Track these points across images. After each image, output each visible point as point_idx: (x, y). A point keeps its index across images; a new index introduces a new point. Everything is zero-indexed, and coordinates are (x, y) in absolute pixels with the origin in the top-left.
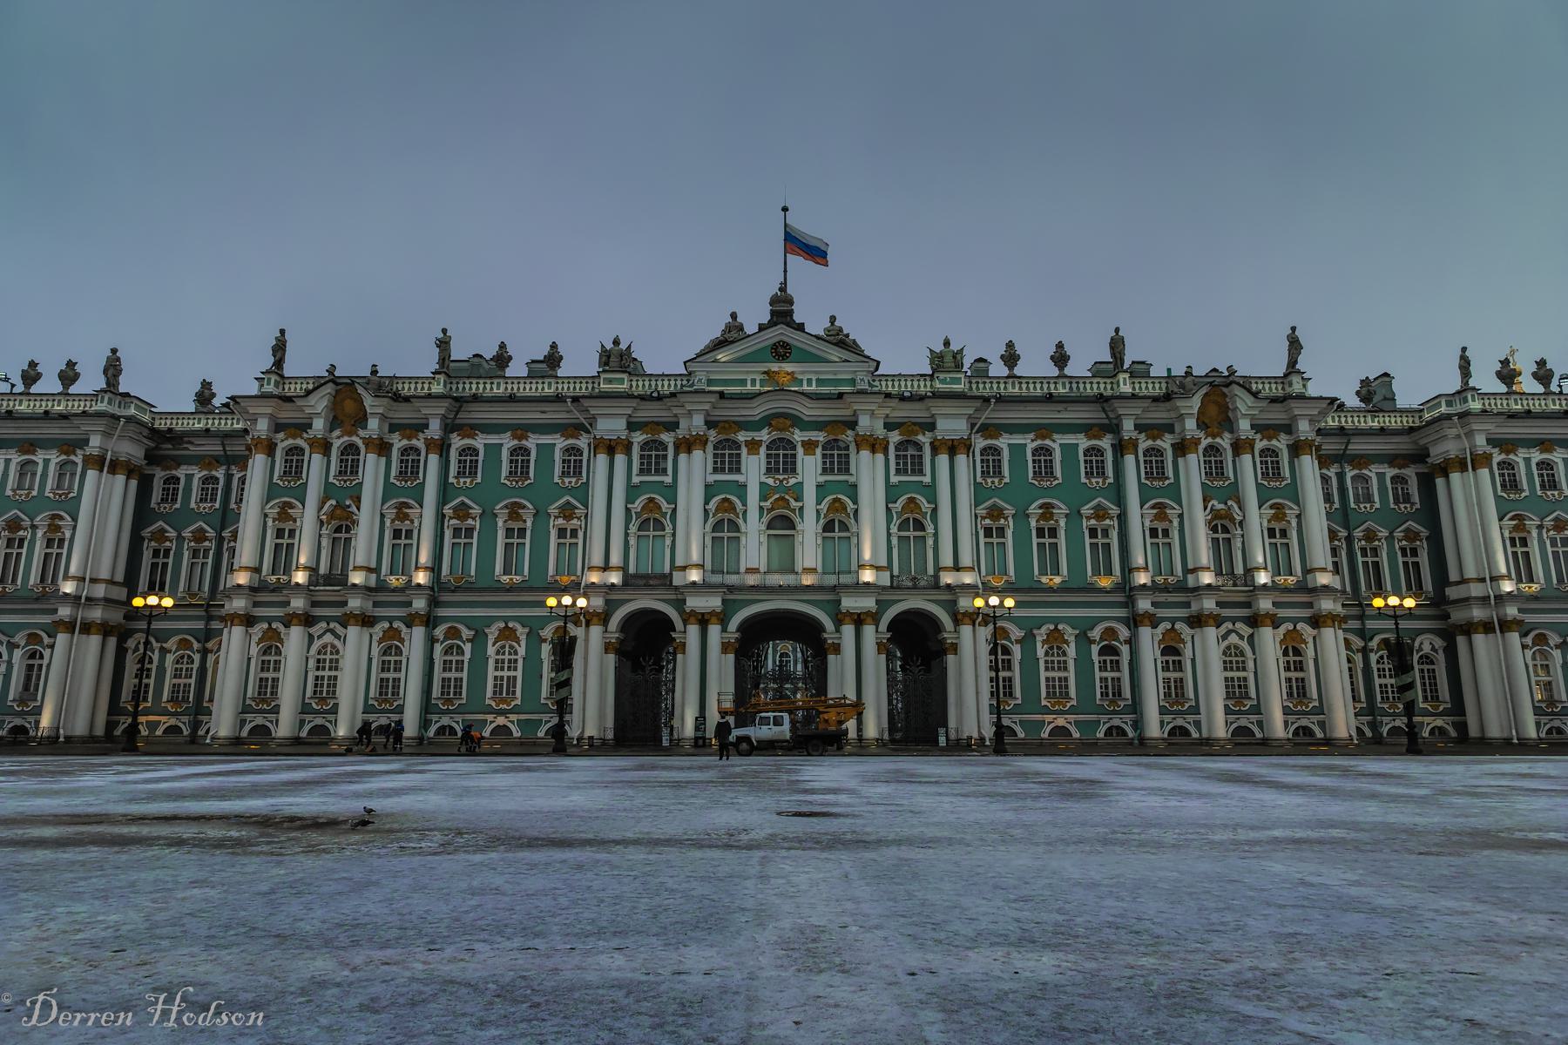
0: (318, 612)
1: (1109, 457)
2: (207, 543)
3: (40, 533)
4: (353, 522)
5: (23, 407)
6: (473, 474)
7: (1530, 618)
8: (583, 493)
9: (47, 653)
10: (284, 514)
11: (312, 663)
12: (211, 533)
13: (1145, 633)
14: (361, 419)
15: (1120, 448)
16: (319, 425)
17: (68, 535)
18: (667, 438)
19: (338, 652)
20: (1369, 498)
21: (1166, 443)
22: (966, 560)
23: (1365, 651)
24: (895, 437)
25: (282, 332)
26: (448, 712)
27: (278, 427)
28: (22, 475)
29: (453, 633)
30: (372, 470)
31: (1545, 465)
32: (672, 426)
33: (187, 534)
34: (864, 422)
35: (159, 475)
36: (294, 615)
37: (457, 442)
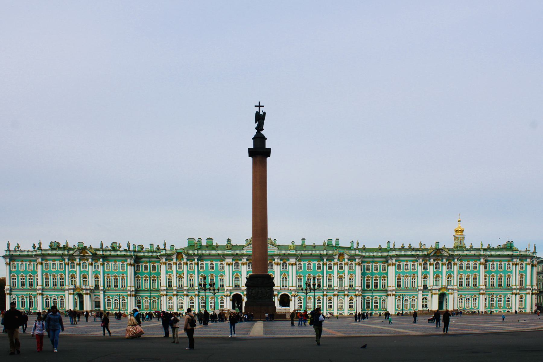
1: (322, 265)
6: (203, 269)
7: (396, 294)
8: (224, 272)
10: (170, 276)
13: (325, 297)
15: (323, 264)
16: (174, 260)
18: (239, 262)
20: (377, 269)
21: (332, 263)
22: (294, 285)
23: (372, 299)
24: (282, 262)
30: (185, 268)
31: (407, 265)
32: (240, 260)
34: (276, 260)
37: (200, 263)
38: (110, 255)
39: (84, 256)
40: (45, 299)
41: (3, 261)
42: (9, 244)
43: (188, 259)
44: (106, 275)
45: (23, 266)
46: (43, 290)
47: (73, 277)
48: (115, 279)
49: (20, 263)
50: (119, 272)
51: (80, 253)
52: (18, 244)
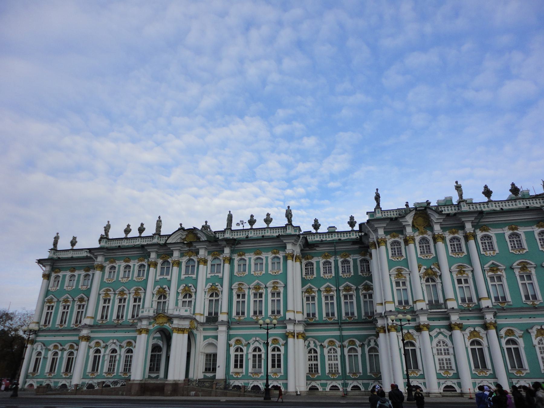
0: (432, 323)
2: (332, 293)
3: (269, 290)
4: (437, 276)
5: (251, 235)
6: (492, 249)
9: (282, 348)
10: (399, 273)
11: (435, 351)
12: (334, 288)
14: (429, 226)
17: (282, 290)
19: (447, 345)
25: (377, 190)
26: (521, 378)
27: (386, 233)
28: (256, 264)
29: (510, 332)
33: (322, 288)
35: (304, 262)
36: (424, 325)
37: (479, 234)
38: (247, 239)
39: (190, 244)
40: (92, 351)
41: (39, 271)
42: (56, 239)
43: (444, 229)
44: (235, 285)
45: (68, 280)
46: (90, 326)
47: (162, 294)
48: (255, 295)
49: (68, 274)
50: (267, 276)
51: (184, 239)
52: (74, 238)
